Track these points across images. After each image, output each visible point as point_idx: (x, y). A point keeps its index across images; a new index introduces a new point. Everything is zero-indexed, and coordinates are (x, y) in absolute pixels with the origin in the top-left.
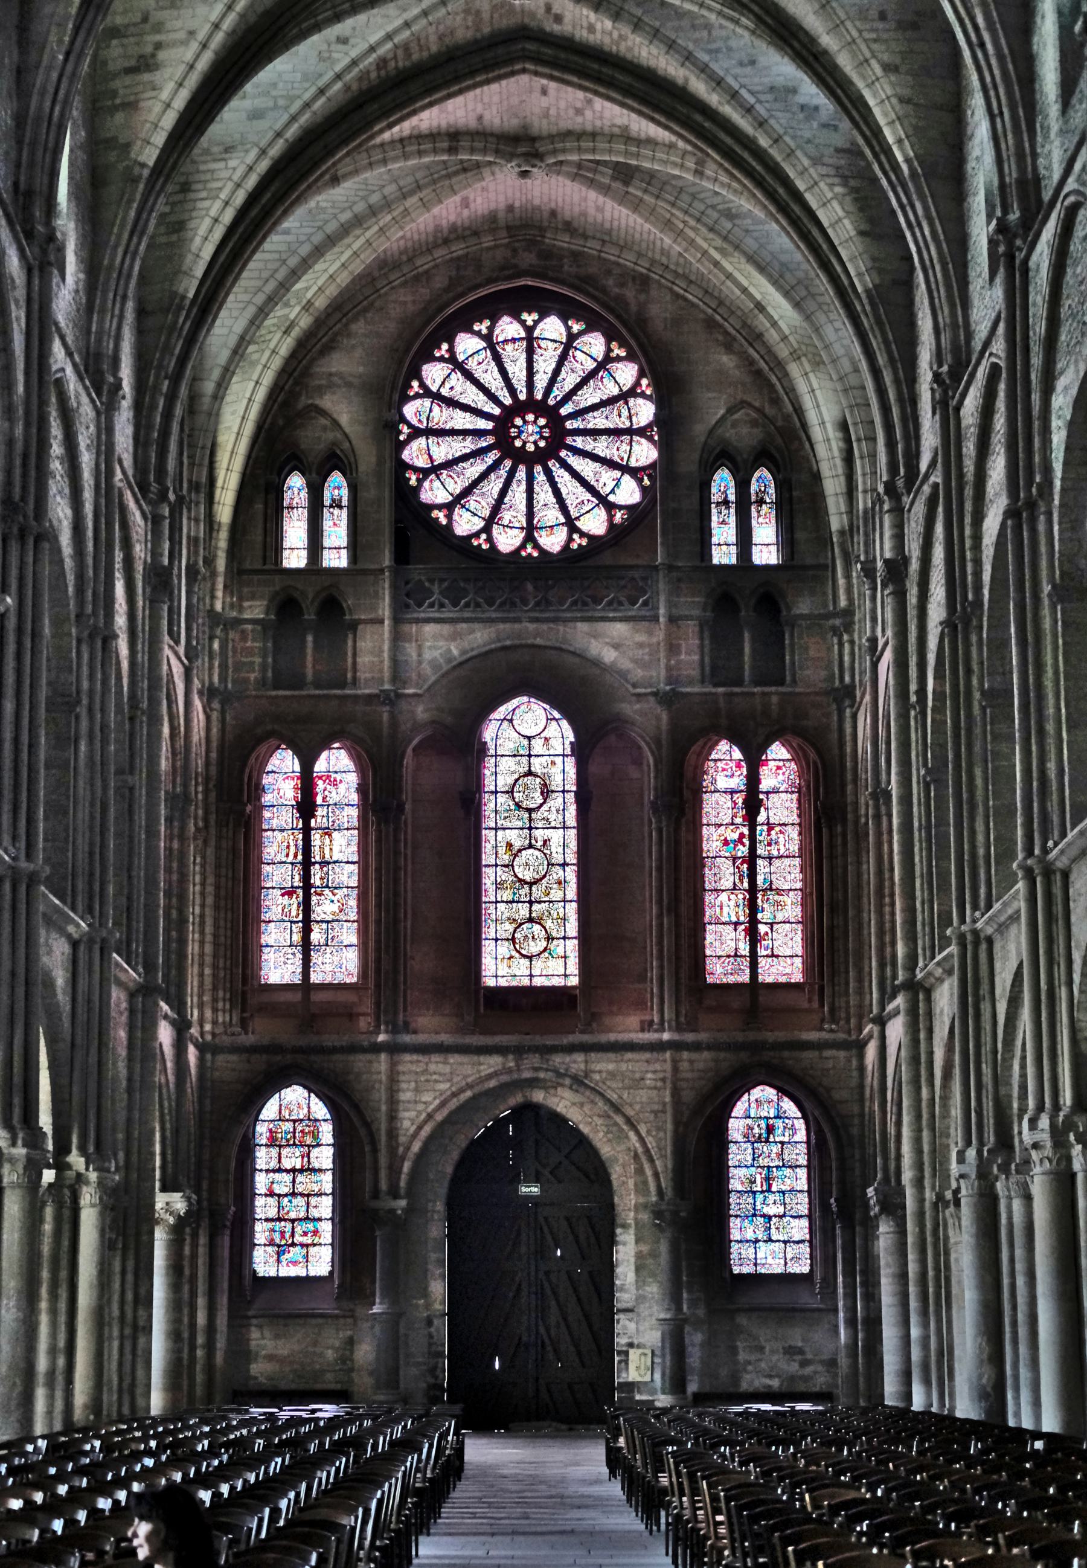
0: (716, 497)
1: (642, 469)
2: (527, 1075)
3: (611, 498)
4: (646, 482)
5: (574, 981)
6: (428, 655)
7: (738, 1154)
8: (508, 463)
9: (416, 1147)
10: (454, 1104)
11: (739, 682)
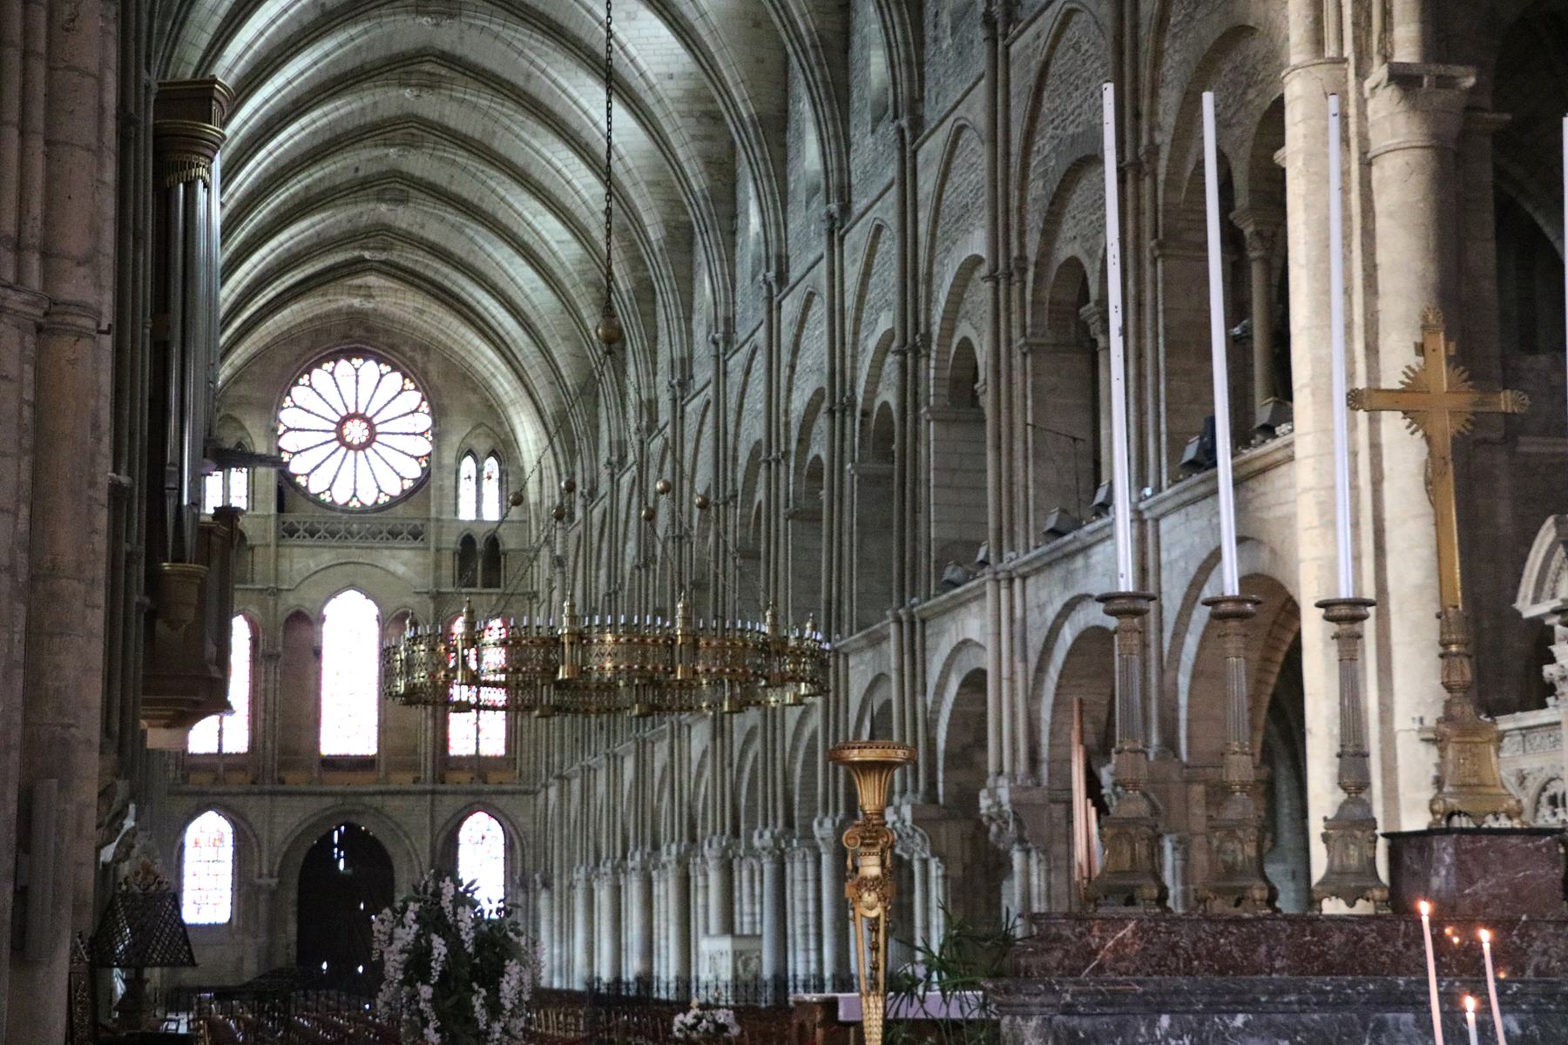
2: (348, 807)
6: (296, 567)
9: (284, 849)
10: (305, 825)
11: (474, 585)
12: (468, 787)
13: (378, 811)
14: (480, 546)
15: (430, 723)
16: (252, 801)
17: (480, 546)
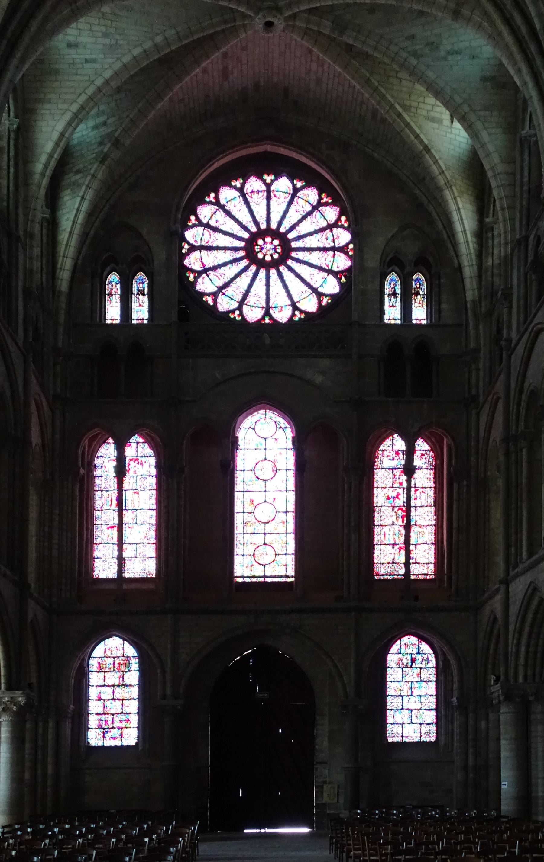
1: (341, 272)
3: (320, 290)
4: (343, 280)
8: (253, 268)
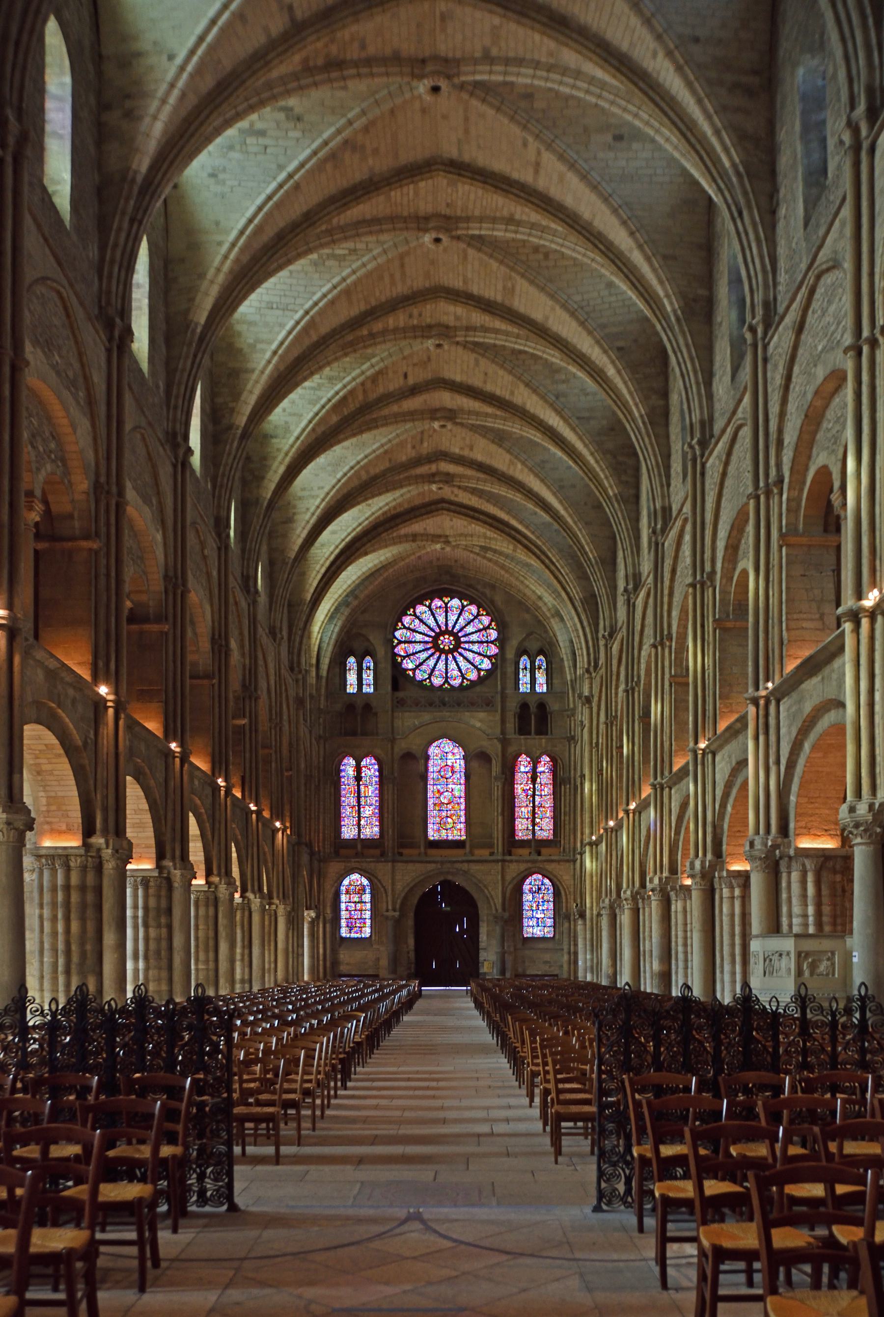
0: (521, 666)
5: (464, 838)
7: (527, 897)
12: (528, 858)
13: (465, 872)
14: (533, 708)
15: (500, 818)
16: (380, 866)
17: (533, 708)
